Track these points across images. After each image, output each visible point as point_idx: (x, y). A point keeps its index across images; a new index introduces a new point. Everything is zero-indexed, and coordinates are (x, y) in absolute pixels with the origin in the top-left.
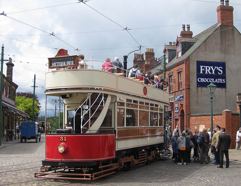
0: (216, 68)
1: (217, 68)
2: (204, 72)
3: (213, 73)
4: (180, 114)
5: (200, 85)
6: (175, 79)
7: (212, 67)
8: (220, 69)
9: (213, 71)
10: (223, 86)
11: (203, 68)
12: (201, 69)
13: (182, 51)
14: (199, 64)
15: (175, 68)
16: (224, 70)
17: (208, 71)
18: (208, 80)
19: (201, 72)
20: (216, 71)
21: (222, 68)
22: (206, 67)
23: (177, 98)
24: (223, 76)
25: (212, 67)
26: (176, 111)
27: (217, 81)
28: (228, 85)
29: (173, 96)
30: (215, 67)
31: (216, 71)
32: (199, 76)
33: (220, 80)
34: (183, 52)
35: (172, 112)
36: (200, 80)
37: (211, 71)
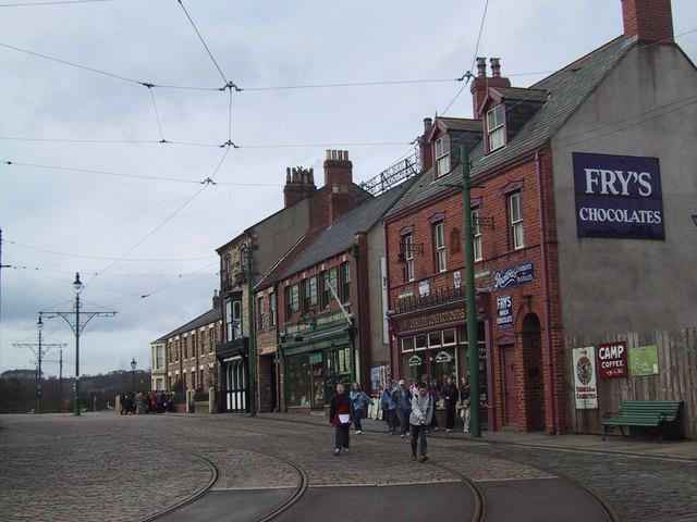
0: (633, 177)
1: (635, 174)
2: (596, 188)
3: (625, 192)
4: (520, 329)
5: (588, 231)
6: (493, 218)
7: (620, 173)
8: (644, 178)
9: (625, 184)
10: (654, 233)
11: (594, 175)
12: (589, 181)
13: (452, 158)
14: (582, 161)
15: (494, 182)
16: (656, 181)
17: (607, 186)
18: (612, 216)
19: (589, 190)
20: (633, 185)
21: (648, 175)
22: (604, 172)
23: (506, 278)
24: (656, 201)
25: (620, 173)
26: (500, 321)
27: (637, 218)
28: (669, 231)
29: (488, 273)
30: (630, 173)
31: (633, 185)
32: (583, 199)
33: (646, 216)
34: (511, 132)
35: (487, 322)
36: (586, 215)
37: (618, 185)
